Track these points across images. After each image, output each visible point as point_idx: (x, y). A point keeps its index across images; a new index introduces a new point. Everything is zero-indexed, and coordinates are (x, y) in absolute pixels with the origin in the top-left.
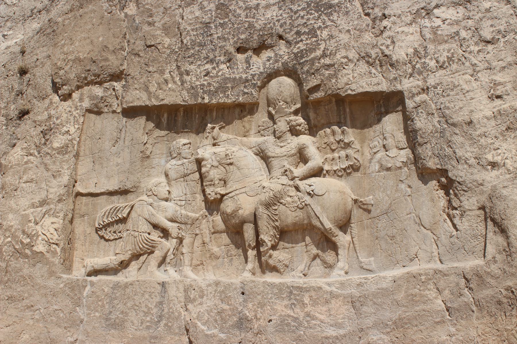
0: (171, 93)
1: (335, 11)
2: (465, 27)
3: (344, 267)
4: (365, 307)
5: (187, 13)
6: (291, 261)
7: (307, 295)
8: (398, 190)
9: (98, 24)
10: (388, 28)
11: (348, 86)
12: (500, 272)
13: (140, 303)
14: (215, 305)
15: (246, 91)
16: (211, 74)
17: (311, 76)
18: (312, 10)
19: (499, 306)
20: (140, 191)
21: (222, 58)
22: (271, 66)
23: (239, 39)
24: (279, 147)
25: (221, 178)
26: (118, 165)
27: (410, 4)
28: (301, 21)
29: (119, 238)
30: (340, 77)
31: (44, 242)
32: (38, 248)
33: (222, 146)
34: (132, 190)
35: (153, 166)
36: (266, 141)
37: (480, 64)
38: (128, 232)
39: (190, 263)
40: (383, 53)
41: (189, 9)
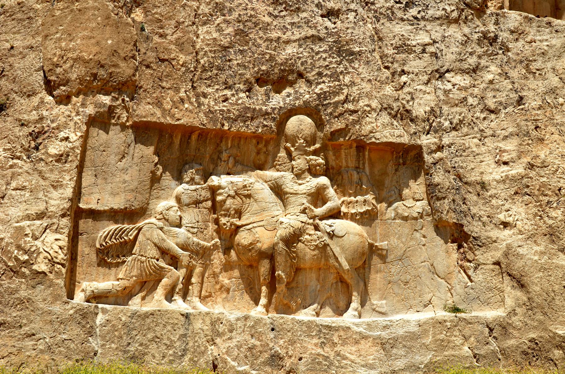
0: (188, 113)
1: (356, 59)
2: (471, 94)
4: (395, 349)
5: (203, 32)
7: (336, 334)
8: (413, 239)
9: (104, 24)
10: (408, 83)
11: (372, 134)
12: (521, 324)
13: (162, 335)
14: (245, 340)
15: (265, 123)
16: (230, 101)
18: (333, 53)
19: (524, 356)
21: (242, 86)
22: (292, 102)
23: (259, 69)
24: (297, 184)
26: (125, 182)
27: (426, 65)
28: (322, 63)
31: (47, 261)
32: (39, 267)
36: (282, 176)
37: (486, 131)
38: (133, 256)
40: (404, 107)
41: (205, 28)
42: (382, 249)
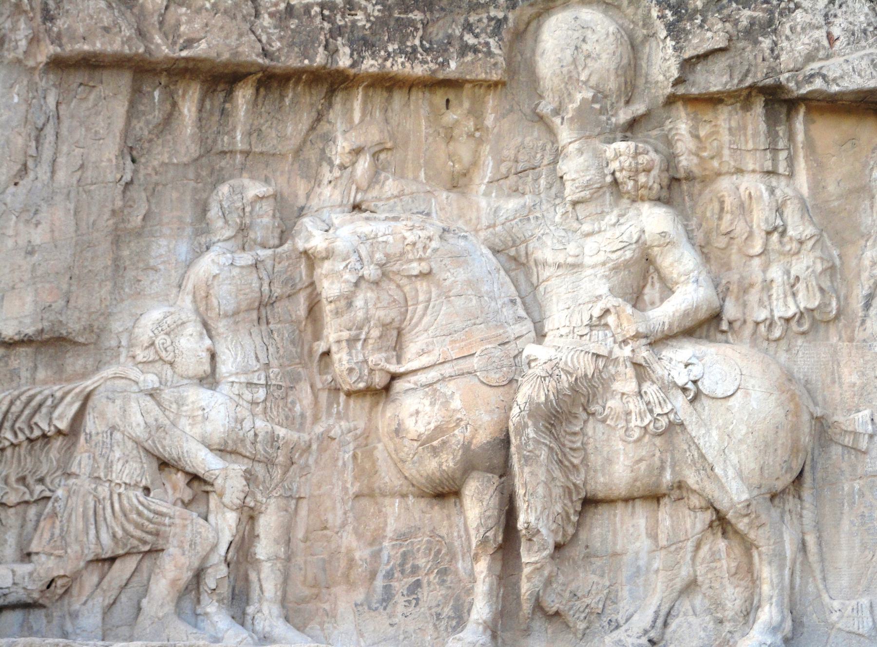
3: (783, 620)
6: (611, 598)
11: (815, 66)
15: (470, 39)
17: (692, 18)
20: (107, 344)
25: (388, 320)
29: (36, 501)
30: (788, 32)
33: (387, 215)
34: (81, 340)
35: (152, 262)
38: (72, 481)
39: (279, 593)
42: (856, 434)
